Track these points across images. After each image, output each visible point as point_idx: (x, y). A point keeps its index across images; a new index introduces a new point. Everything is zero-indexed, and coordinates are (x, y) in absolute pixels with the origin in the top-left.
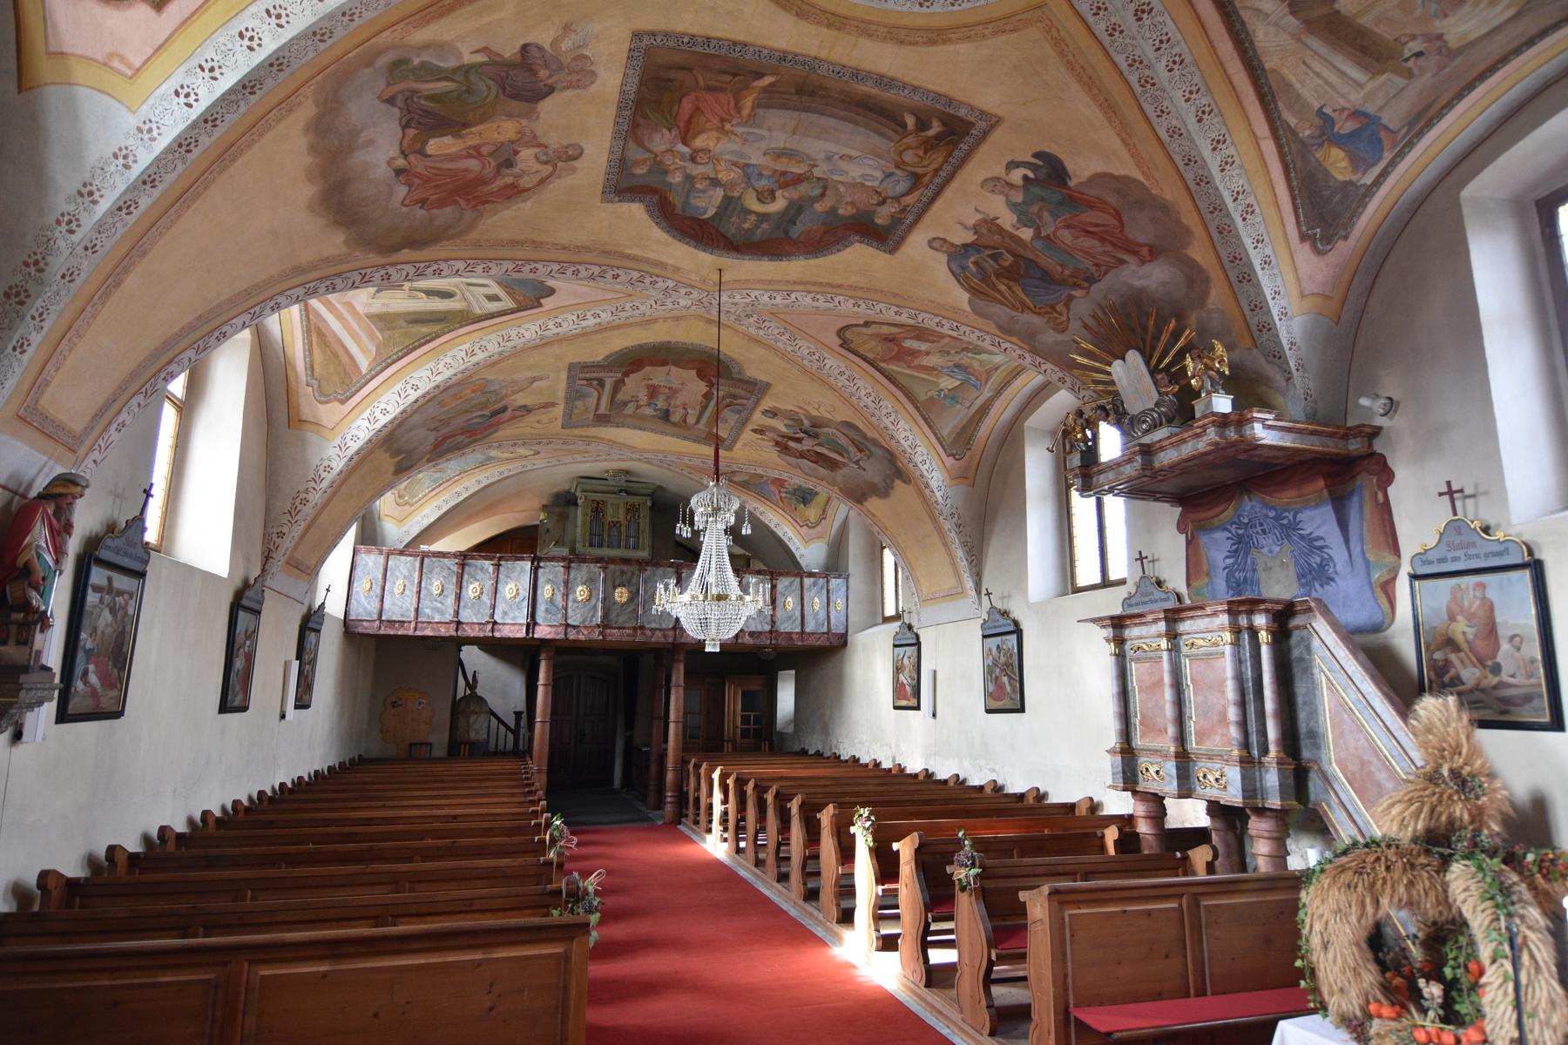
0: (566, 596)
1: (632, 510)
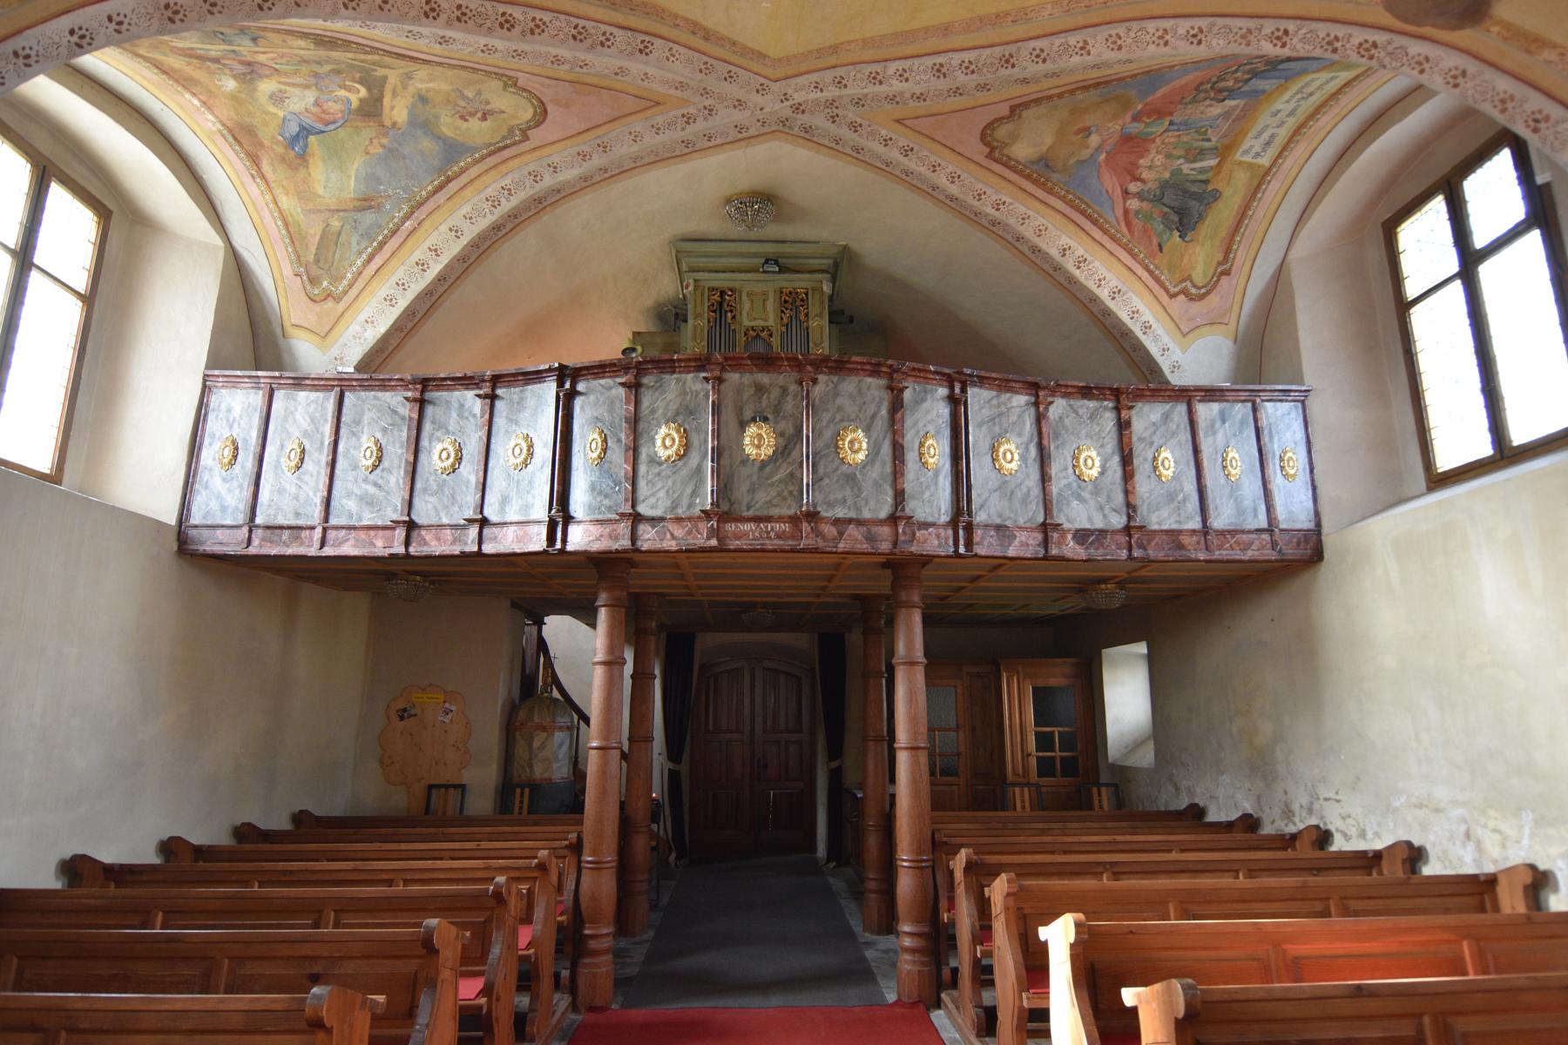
0: (634, 450)
1: (792, 303)
